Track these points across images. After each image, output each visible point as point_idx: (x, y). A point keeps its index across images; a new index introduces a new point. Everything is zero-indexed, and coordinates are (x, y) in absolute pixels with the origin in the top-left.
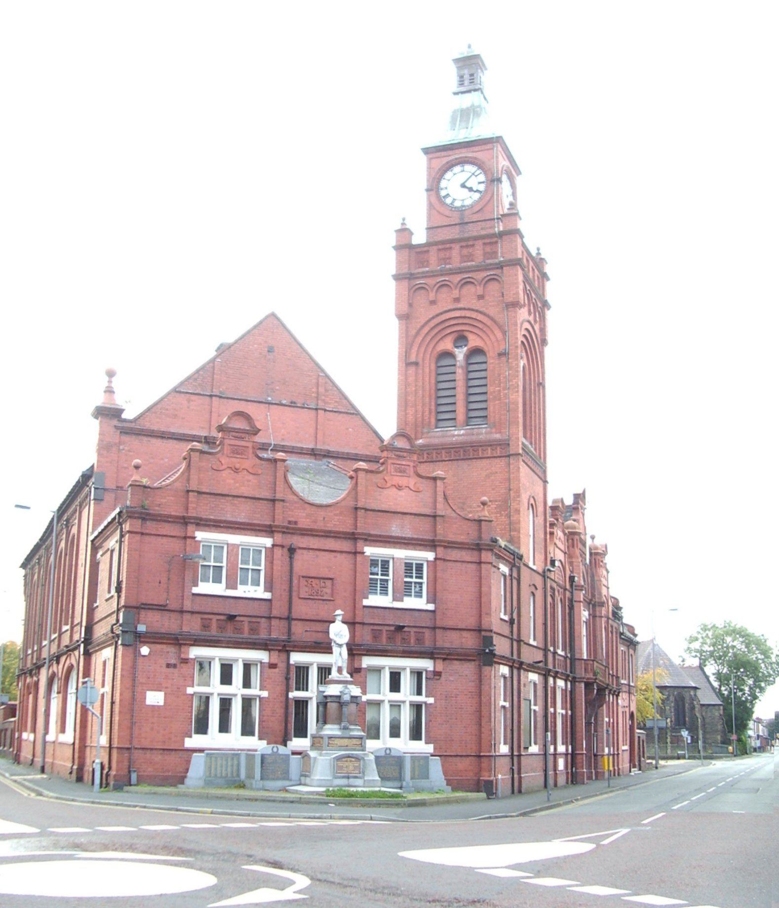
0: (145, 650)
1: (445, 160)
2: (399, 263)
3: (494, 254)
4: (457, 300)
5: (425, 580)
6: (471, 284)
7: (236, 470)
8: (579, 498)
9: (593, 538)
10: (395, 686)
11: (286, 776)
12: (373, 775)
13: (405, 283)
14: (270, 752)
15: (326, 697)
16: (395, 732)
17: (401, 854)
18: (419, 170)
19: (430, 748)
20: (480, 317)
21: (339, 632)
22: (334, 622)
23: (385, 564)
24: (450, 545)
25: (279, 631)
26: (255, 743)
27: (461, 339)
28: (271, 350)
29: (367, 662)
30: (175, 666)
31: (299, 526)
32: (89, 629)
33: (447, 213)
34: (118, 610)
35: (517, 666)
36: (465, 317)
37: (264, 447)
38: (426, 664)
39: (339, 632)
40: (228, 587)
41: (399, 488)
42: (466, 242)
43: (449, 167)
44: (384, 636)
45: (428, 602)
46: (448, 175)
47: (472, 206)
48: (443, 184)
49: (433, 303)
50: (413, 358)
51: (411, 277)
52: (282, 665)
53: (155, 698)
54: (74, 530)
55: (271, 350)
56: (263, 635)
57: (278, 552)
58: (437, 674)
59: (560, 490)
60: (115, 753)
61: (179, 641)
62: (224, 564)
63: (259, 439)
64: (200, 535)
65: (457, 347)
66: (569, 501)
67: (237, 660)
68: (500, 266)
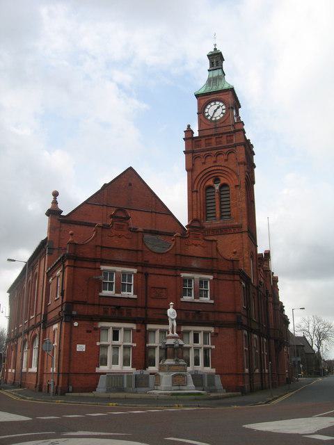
0: (76, 324)
2: (187, 146)
4: (215, 162)
6: (221, 153)
7: (119, 237)
9: (273, 273)
10: (196, 341)
11: (147, 385)
12: (191, 384)
13: (190, 155)
15: (166, 345)
16: (197, 363)
17: (246, 426)
18: (194, 104)
19: (214, 371)
20: (226, 169)
21: (171, 313)
24: (220, 272)
25: (142, 314)
26: (129, 369)
27: (216, 180)
29: (183, 328)
30: (91, 331)
32: (46, 315)
33: (209, 123)
34: (62, 304)
35: (251, 331)
38: (212, 329)
39: (171, 313)
40: (116, 292)
41: (196, 245)
42: (218, 135)
43: (209, 103)
44: (190, 316)
45: (211, 299)
46: (209, 106)
48: (206, 110)
49: (204, 163)
50: (195, 189)
51: (193, 152)
52: (143, 330)
53: (81, 348)
54: (37, 270)
55: (130, 185)
56: (134, 316)
57: (140, 275)
58: (216, 334)
59: (261, 250)
60: (61, 376)
61: (94, 319)
62: (114, 281)
64: (103, 267)
67: (120, 328)
68: (235, 146)
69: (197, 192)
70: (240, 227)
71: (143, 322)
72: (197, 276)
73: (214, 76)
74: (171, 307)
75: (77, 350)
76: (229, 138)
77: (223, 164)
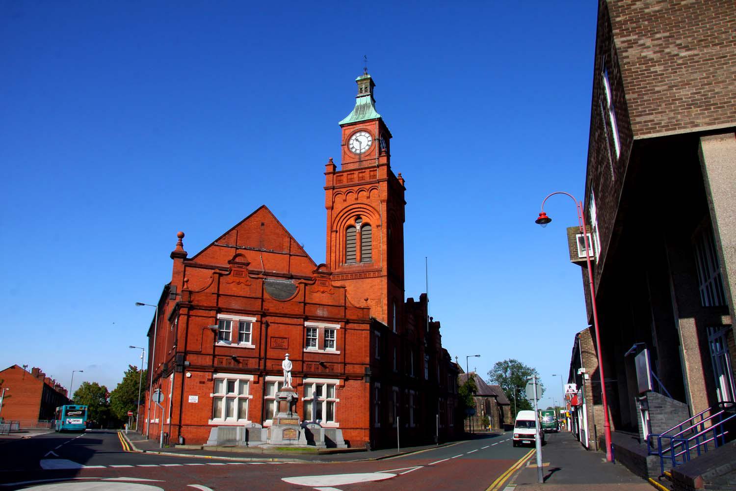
0: (188, 375)
1: (352, 130)
3: (375, 176)
4: (357, 199)
5: (335, 339)
8: (424, 298)
9: (432, 318)
14: (251, 426)
16: (318, 415)
19: (337, 425)
20: (368, 207)
21: (287, 365)
22: (285, 360)
23: (228, 322)
27: (358, 217)
28: (263, 224)
30: (204, 383)
31: (270, 311)
33: (353, 156)
36: (360, 208)
37: (252, 272)
39: (287, 365)
42: (361, 170)
47: (365, 153)
49: (345, 200)
52: (261, 382)
53: (193, 399)
58: (342, 387)
62: (231, 330)
63: (250, 268)
65: (357, 223)
66: (417, 300)
69: (337, 232)
70: (380, 271)
71: (261, 373)
72: (322, 325)
73: (362, 104)
74: (287, 358)
75: (190, 401)
76: (372, 173)
77: (366, 201)
